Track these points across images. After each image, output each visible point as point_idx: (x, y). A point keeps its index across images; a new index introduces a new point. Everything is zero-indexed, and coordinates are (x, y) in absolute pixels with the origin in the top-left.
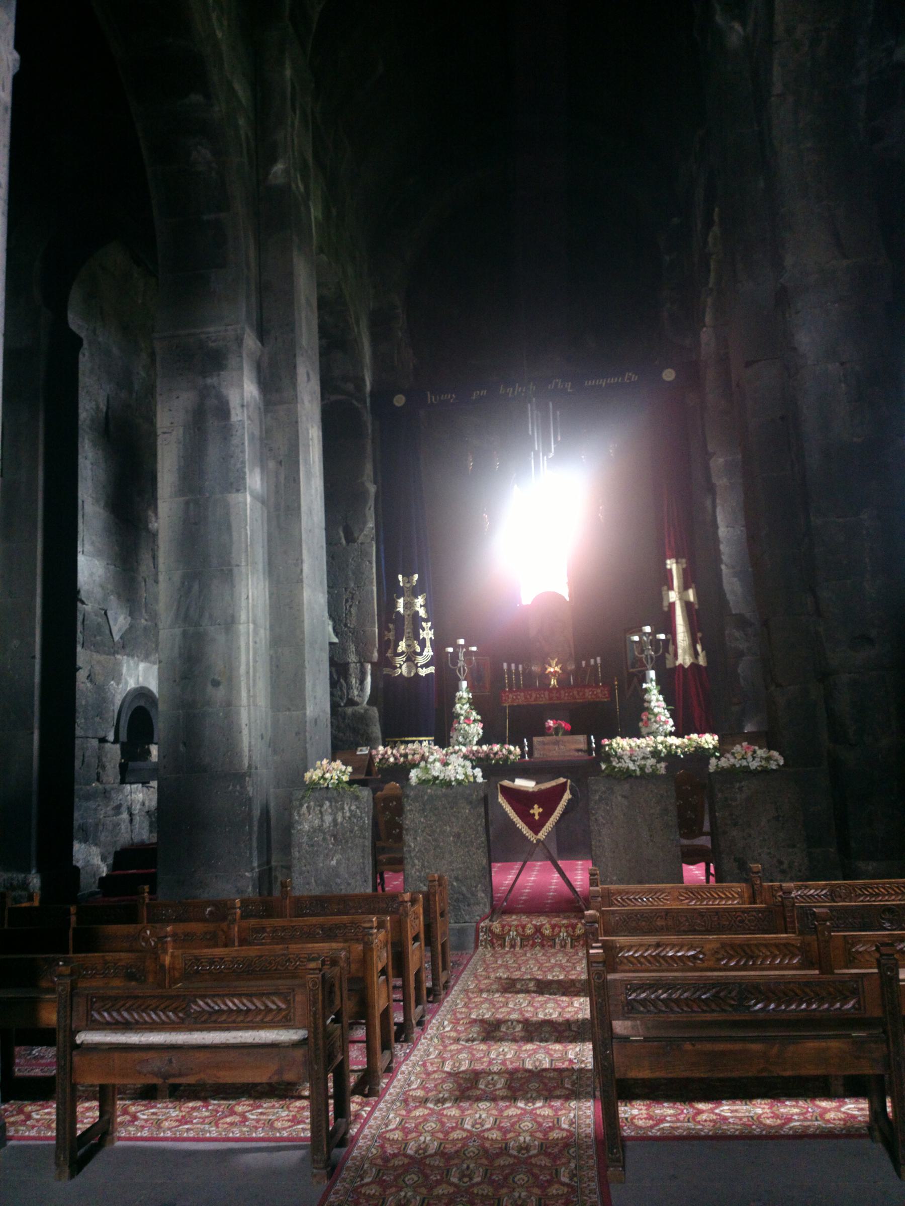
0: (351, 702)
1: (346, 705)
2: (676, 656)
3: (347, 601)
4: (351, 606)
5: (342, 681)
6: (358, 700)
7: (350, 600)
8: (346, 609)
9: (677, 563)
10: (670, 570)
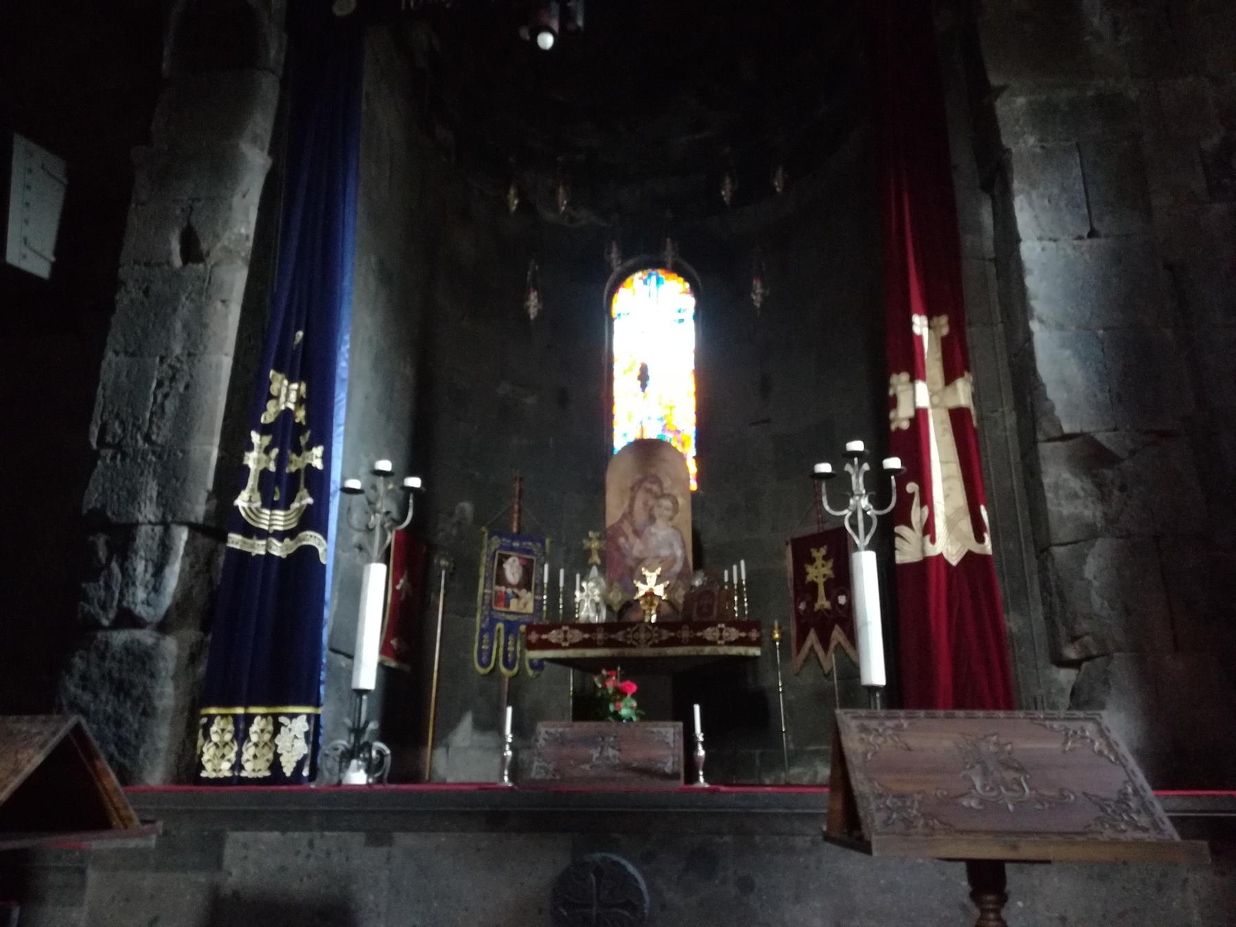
0: (128, 619)
1: (117, 625)
2: (928, 529)
3: (160, 384)
4: (166, 396)
5: (115, 566)
6: (144, 615)
7: (167, 383)
8: (155, 402)
9: (930, 327)
10: (920, 338)
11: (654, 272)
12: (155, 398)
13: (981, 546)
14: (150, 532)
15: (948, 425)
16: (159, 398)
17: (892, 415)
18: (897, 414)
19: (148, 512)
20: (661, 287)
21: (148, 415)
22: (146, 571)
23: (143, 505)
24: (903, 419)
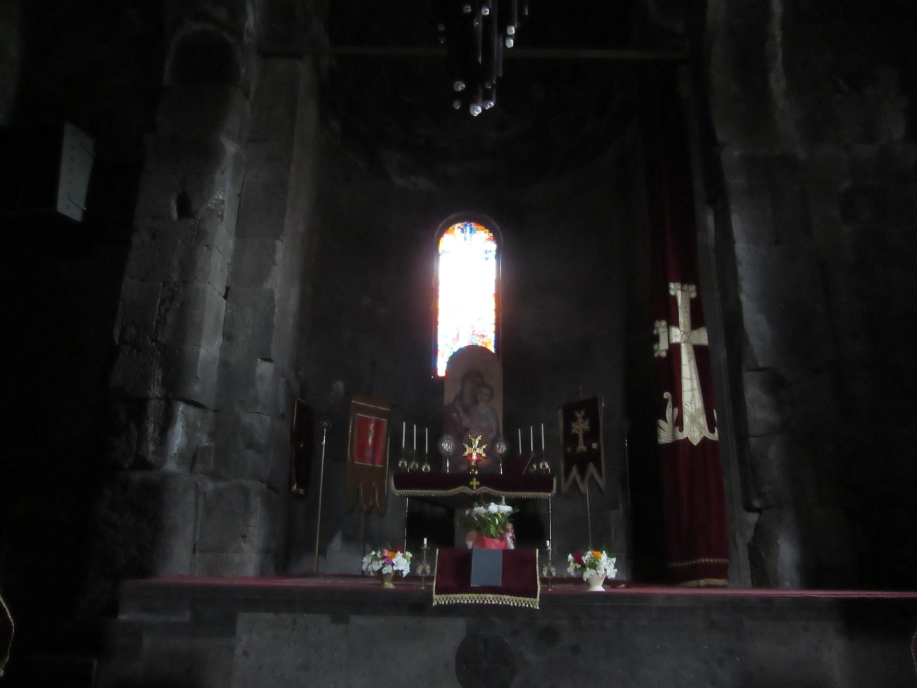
0: (143, 464)
2: (679, 423)
4: (167, 310)
8: (159, 315)
10: (675, 298)
11: (469, 224)
12: (160, 311)
13: (711, 435)
14: (157, 405)
15: (693, 355)
16: (163, 311)
17: (655, 347)
18: (659, 347)
19: (156, 390)
20: (474, 235)
21: (155, 323)
22: (154, 431)
23: (152, 385)
24: (662, 351)
